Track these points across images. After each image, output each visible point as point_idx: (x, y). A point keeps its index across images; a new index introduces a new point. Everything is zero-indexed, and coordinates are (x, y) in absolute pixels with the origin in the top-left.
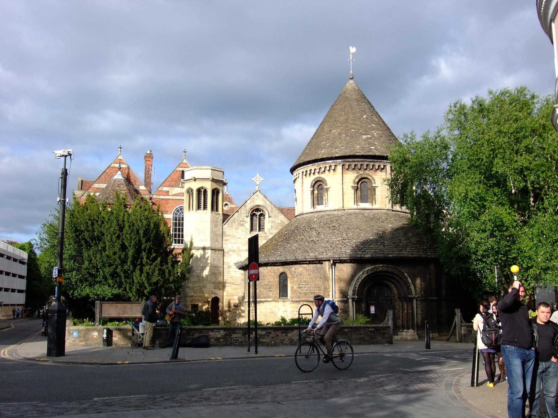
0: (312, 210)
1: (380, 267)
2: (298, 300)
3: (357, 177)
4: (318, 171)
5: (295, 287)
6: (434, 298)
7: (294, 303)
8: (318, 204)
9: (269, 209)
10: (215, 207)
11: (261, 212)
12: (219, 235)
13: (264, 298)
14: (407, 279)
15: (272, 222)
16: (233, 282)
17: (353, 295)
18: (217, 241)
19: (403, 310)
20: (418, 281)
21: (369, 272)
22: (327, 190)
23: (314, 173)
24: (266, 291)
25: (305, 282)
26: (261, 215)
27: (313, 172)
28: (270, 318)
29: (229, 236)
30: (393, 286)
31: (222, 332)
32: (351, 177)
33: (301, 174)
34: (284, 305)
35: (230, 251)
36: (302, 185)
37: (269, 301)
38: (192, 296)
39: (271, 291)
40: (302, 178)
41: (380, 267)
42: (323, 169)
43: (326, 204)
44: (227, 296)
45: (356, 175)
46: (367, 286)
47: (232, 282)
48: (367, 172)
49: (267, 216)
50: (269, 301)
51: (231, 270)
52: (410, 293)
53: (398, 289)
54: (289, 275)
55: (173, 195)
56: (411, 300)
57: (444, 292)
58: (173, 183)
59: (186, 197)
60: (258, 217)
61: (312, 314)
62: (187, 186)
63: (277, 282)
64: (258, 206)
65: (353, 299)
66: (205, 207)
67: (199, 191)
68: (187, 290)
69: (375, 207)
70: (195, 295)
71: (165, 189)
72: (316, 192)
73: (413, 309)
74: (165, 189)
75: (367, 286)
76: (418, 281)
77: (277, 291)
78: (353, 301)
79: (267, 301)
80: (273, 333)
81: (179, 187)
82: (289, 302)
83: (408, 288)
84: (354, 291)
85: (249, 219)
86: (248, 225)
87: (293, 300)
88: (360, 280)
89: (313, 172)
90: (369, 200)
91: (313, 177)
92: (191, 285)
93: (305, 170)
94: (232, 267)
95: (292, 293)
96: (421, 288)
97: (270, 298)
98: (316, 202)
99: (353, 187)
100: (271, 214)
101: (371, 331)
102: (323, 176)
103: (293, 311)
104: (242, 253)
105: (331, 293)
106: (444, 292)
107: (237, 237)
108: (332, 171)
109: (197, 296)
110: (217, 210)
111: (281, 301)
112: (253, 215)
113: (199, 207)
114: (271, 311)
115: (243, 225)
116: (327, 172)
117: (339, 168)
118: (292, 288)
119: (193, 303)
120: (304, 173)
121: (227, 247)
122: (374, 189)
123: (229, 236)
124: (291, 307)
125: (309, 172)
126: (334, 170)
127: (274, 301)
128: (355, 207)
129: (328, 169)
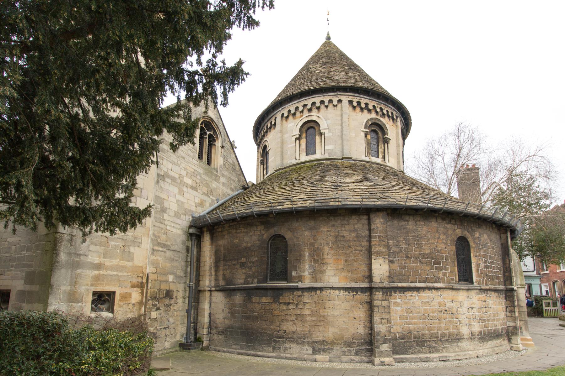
2: (487, 287)
4: (378, 110)
5: (482, 265)
7: (482, 294)
11: (212, 133)
13: (420, 282)
16: (168, 243)
23: (369, 111)
24: (428, 268)
26: (210, 136)
27: (371, 107)
28: (440, 323)
34: (468, 297)
36: (348, 117)
37: (437, 289)
39: (437, 268)
42: (385, 112)
44: (156, 273)
47: (166, 243)
49: (218, 143)
50: (437, 289)
51: (166, 216)
60: (207, 136)
63: (452, 253)
77: (454, 270)
79: (430, 289)
82: (475, 291)
87: (484, 287)
94: (168, 210)
95: (478, 276)
97: (438, 281)
103: (481, 308)
104: (185, 189)
111: (463, 289)
114: (443, 308)
118: (478, 265)
120: (355, 104)
124: (479, 300)
127: (452, 289)
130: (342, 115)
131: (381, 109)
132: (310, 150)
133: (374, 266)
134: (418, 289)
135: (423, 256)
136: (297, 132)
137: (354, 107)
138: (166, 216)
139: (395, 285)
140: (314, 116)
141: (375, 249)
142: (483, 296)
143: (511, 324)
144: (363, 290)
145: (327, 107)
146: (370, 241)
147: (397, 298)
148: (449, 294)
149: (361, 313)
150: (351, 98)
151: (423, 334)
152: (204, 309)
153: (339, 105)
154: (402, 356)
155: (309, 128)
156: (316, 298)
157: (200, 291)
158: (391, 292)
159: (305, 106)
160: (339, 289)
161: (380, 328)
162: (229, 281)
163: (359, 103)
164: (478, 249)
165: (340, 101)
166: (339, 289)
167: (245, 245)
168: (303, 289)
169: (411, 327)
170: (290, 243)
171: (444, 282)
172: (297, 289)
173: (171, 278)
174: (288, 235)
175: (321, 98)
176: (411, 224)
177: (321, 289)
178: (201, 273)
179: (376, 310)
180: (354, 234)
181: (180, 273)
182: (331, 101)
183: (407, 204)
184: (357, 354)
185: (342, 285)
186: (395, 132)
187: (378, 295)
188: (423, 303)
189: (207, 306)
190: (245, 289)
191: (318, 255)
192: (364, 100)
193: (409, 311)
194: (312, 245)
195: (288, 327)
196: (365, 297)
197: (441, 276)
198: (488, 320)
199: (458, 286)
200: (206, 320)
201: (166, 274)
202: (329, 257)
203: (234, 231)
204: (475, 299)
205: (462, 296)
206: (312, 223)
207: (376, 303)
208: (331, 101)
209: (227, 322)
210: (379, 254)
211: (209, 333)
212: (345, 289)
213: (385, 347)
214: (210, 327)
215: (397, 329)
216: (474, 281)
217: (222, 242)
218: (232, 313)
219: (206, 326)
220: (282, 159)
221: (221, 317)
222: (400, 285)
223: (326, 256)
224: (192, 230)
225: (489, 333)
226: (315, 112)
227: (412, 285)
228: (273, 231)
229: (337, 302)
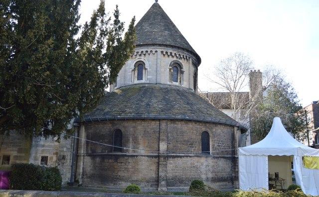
0: (169, 83)
2: (218, 156)
4: (178, 56)
22: (182, 72)
23: (173, 57)
25: (222, 141)
27: (173, 55)
34: (206, 161)
37: (190, 157)
38: (43, 146)
39: (191, 147)
42: (182, 56)
43: (180, 82)
50: (190, 157)
54: (211, 135)
79: (187, 156)
102: (180, 60)
109: (47, 147)
118: (213, 145)
119: (43, 155)
120: (164, 53)
125: (169, 54)
130: (157, 59)
131: (180, 55)
132: (140, 77)
133: (160, 146)
134: (181, 157)
135: (184, 141)
136: (133, 67)
137: (164, 55)
139: (170, 154)
140: (142, 59)
141: (161, 138)
142: (216, 160)
143: (233, 175)
144: (155, 157)
145: (149, 54)
146: (159, 134)
147: (171, 161)
148: (196, 159)
149: (154, 167)
150: (162, 50)
151: (182, 178)
152: (80, 166)
153: (156, 53)
154: (172, 187)
155: (140, 64)
156: (134, 160)
157: (78, 156)
158: (168, 158)
159: (138, 52)
160: (145, 156)
161: (162, 174)
162: (93, 151)
163: (167, 53)
164: (214, 136)
165: (156, 51)
166: (145, 156)
167: (102, 133)
168: (128, 156)
169: (177, 174)
170: (123, 133)
171: (194, 153)
172: (126, 156)
173: (65, 149)
174: (123, 130)
175: (146, 50)
176: (179, 125)
177: (137, 156)
178: (79, 146)
179: (160, 166)
180: (153, 131)
181: (69, 147)
182: (151, 51)
183: (176, 117)
184: (151, 186)
185: (146, 154)
186: (188, 67)
187: (162, 159)
188: (183, 163)
189: (82, 164)
190: (101, 155)
191: (136, 140)
192: (170, 50)
193: (176, 167)
194: (134, 135)
195: (121, 174)
196: (156, 160)
197: (193, 150)
198: (218, 172)
199: (201, 155)
200: (81, 171)
201: (63, 147)
202: (141, 141)
203: (97, 126)
205: (203, 160)
206: (134, 124)
207: (160, 163)
208: (151, 51)
209: (92, 171)
210: (163, 140)
211: (82, 178)
212: (148, 156)
213: (163, 183)
214: (83, 175)
215: (170, 175)
216: (211, 151)
217: (90, 131)
218: (95, 167)
219: (81, 174)
220: (125, 81)
221: (89, 169)
222: (172, 154)
223: (139, 141)
224: (75, 124)
225: (218, 178)
226: (143, 57)
227: (178, 155)
228: (115, 127)
229: (143, 162)
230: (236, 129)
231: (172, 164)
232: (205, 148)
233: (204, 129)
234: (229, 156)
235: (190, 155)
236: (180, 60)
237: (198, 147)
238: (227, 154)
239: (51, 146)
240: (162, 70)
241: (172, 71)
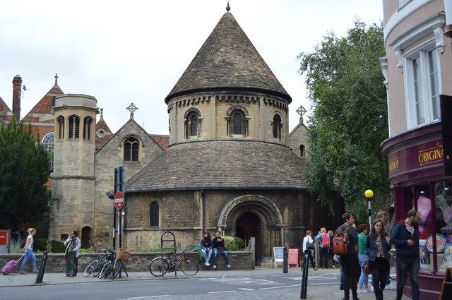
0: (184, 140)
1: (249, 197)
3: (230, 109)
4: (191, 102)
6: (301, 227)
8: (192, 135)
9: (144, 139)
10: (87, 136)
12: (91, 164)
14: (275, 209)
15: (146, 151)
17: (223, 223)
18: (88, 170)
19: (271, 239)
20: (286, 211)
21: (239, 202)
23: (188, 104)
27: (187, 102)
29: (101, 165)
30: (261, 216)
31: (88, 258)
32: (225, 108)
33: (175, 104)
35: (102, 180)
37: (140, 230)
38: (62, 226)
40: (176, 108)
41: (249, 197)
42: (197, 101)
45: (229, 107)
46: (237, 215)
48: (240, 104)
49: (141, 146)
50: (140, 230)
51: (103, 199)
52: (278, 222)
53: (266, 219)
54: (160, 205)
55: (44, 122)
56: (279, 229)
57: (311, 221)
58: (44, 109)
59: (56, 125)
61: (175, 241)
62: (58, 114)
64: (133, 135)
65: (223, 228)
66: (77, 136)
67: (71, 119)
68: (57, 220)
69: (247, 138)
70: (65, 225)
71: (35, 115)
72: (190, 123)
73: (280, 238)
74: (35, 115)
75: (237, 215)
76: (286, 211)
78: (222, 230)
80: (139, 259)
81: (50, 113)
83: (276, 216)
84: (224, 220)
85: (122, 148)
86: (121, 154)
88: (230, 210)
89: (187, 102)
90: (242, 131)
91: (187, 108)
92: (60, 215)
93: (179, 101)
96: (290, 218)
98: (189, 133)
99: (226, 118)
100: (145, 144)
101: (234, 258)
102: (196, 107)
105: (201, 222)
106: (311, 221)
107: (110, 165)
108: (205, 103)
109: (66, 226)
110: (89, 138)
112: (127, 146)
113: (71, 136)
115: (116, 154)
116: (200, 103)
117: (213, 100)
121: (100, 176)
122: (247, 121)
123: (101, 165)
125: (183, 103)
126: (208, 102)
127: (145, 230)
128: (228, 138)
129: (202, 100)
138: (103, 199)
147: (129, 235)
148: (145, 233)
163: (181, 102)
204: (159, 234)
205: (151, 234)
230: (197, 196)
231: (131, 238)
232: (154, 222)
233: (153, 200)
234: (186, 228)
235: (140, 229)
236: (196, 107)
237: (147, 220)
238: (185, 226)
239: (69, 226)
240: (179, 125)
241: (190, 123)
